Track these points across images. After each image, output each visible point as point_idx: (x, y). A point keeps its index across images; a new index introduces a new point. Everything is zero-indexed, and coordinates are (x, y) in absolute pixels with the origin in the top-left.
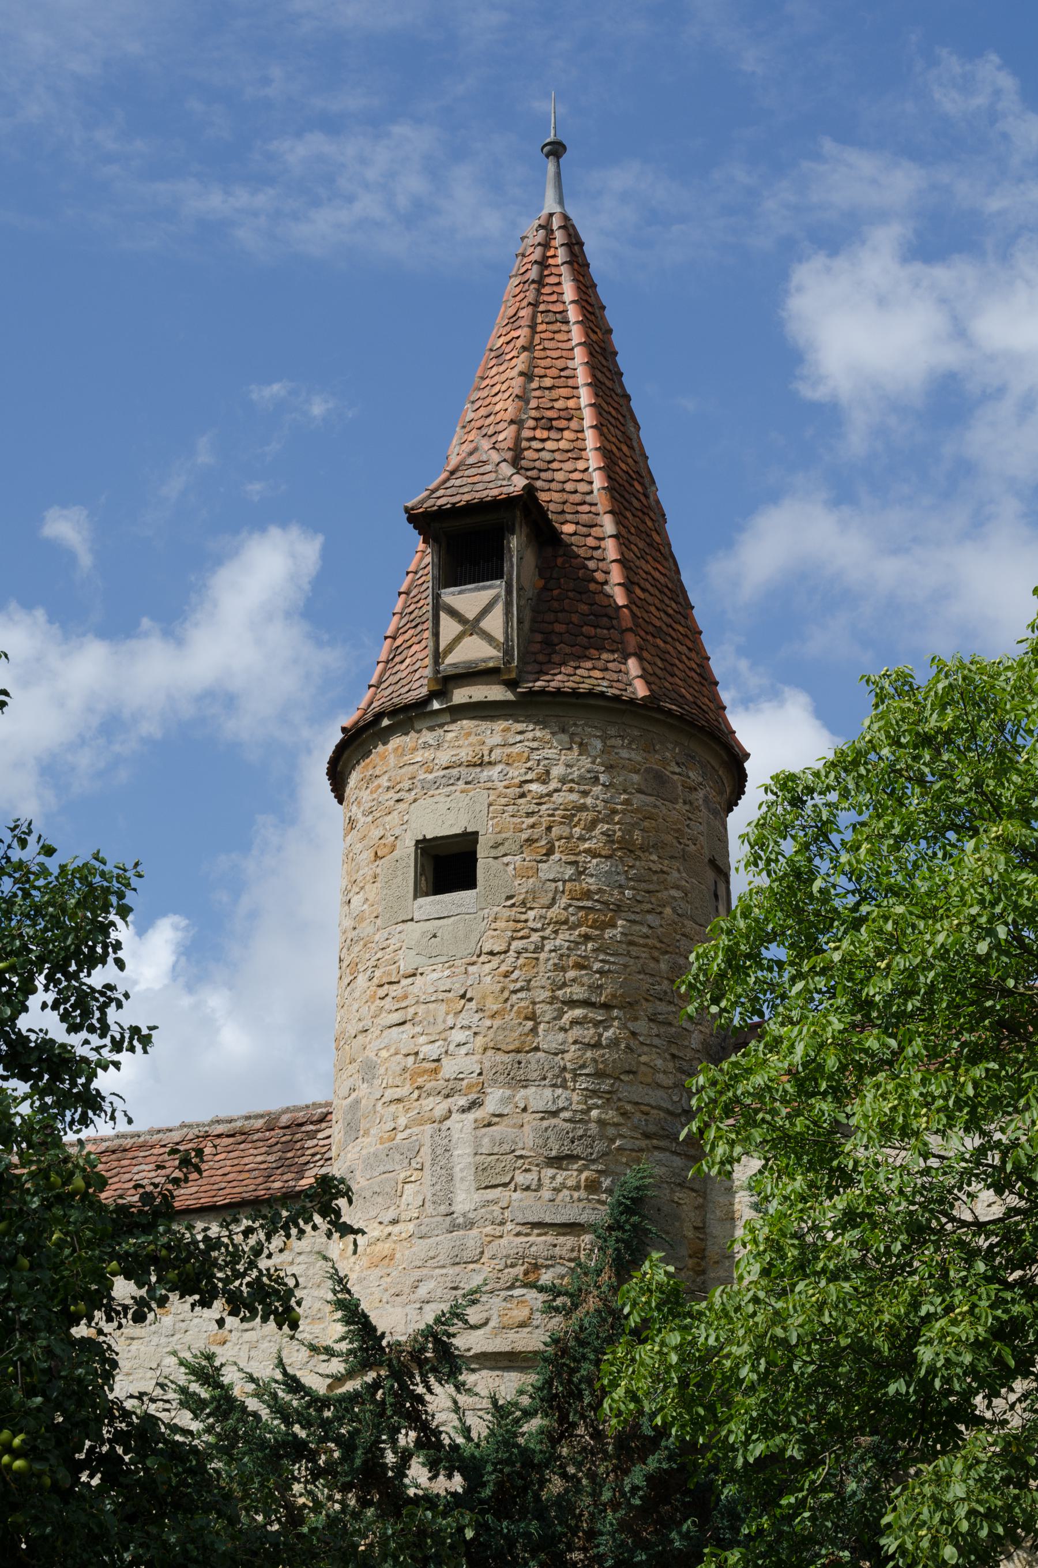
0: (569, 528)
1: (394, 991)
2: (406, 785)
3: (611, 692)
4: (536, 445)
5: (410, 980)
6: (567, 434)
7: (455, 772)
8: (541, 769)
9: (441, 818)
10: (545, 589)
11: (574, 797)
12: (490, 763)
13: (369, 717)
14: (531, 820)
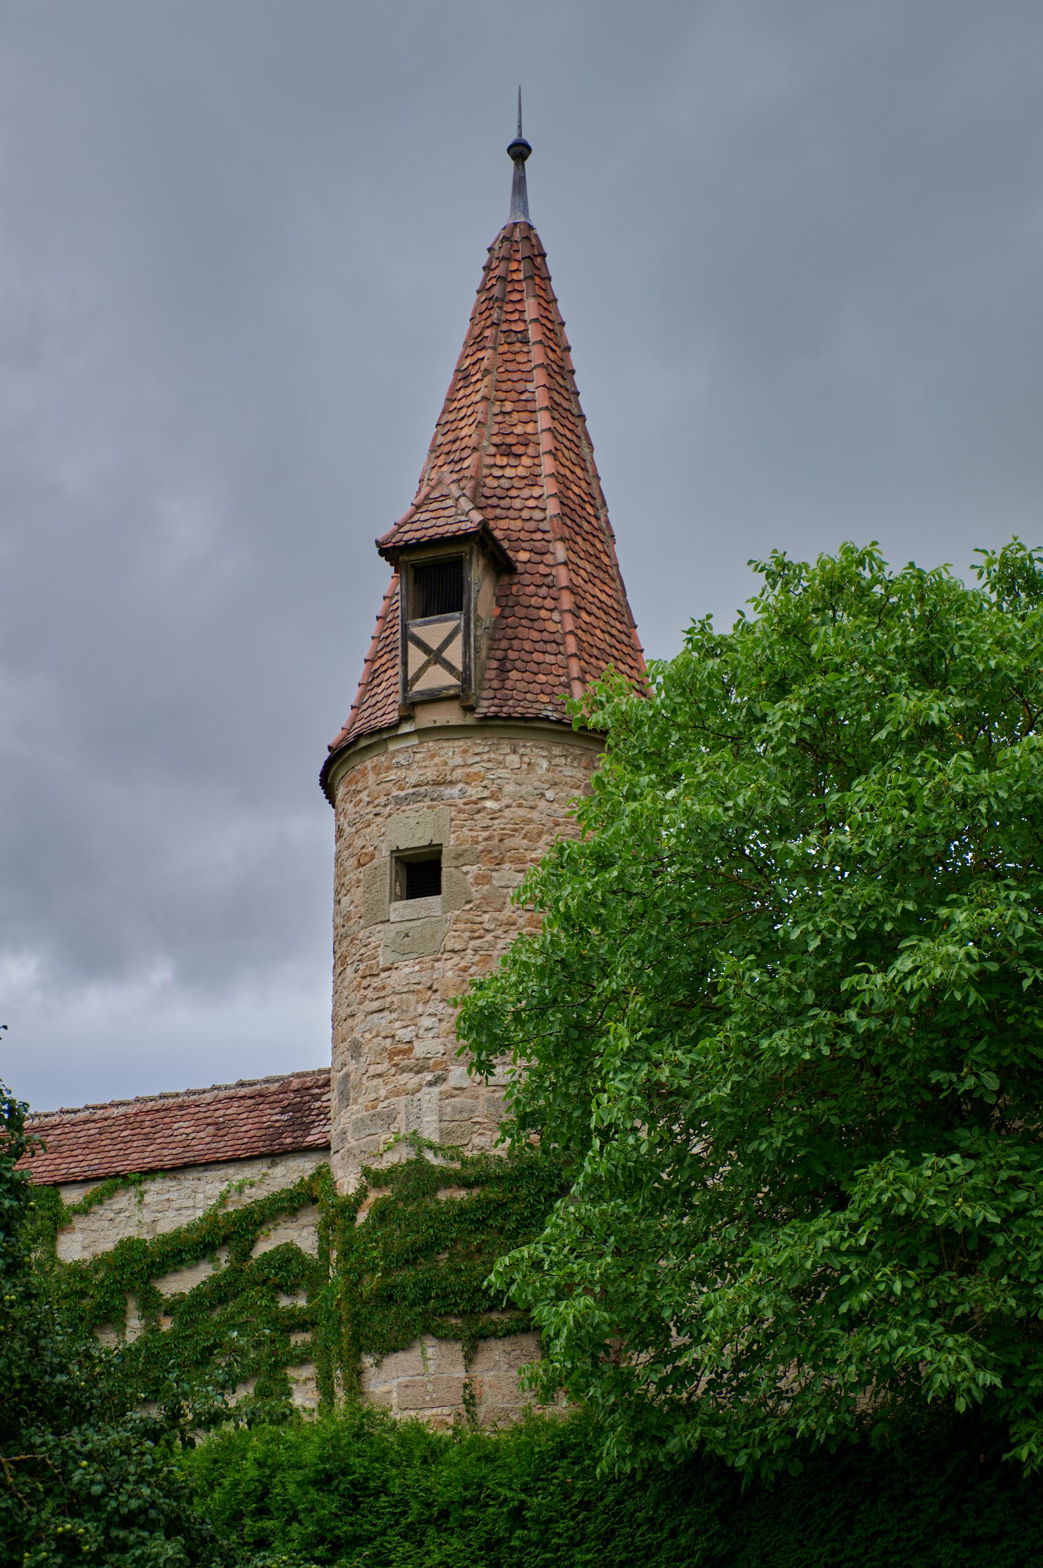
0: (523, 556)
1: (376, 982)
2: (382, 800)
3: (555, 716)
4: (497, 472)
5: (387, 974)
6: (526, 461)
7: (422, 790)
8: (494, 788)
9: (412, 831)
10: (502, 616)
11: (521, 812)
12: (451, 782)
13: (351, 737)
14: (486, 834)
